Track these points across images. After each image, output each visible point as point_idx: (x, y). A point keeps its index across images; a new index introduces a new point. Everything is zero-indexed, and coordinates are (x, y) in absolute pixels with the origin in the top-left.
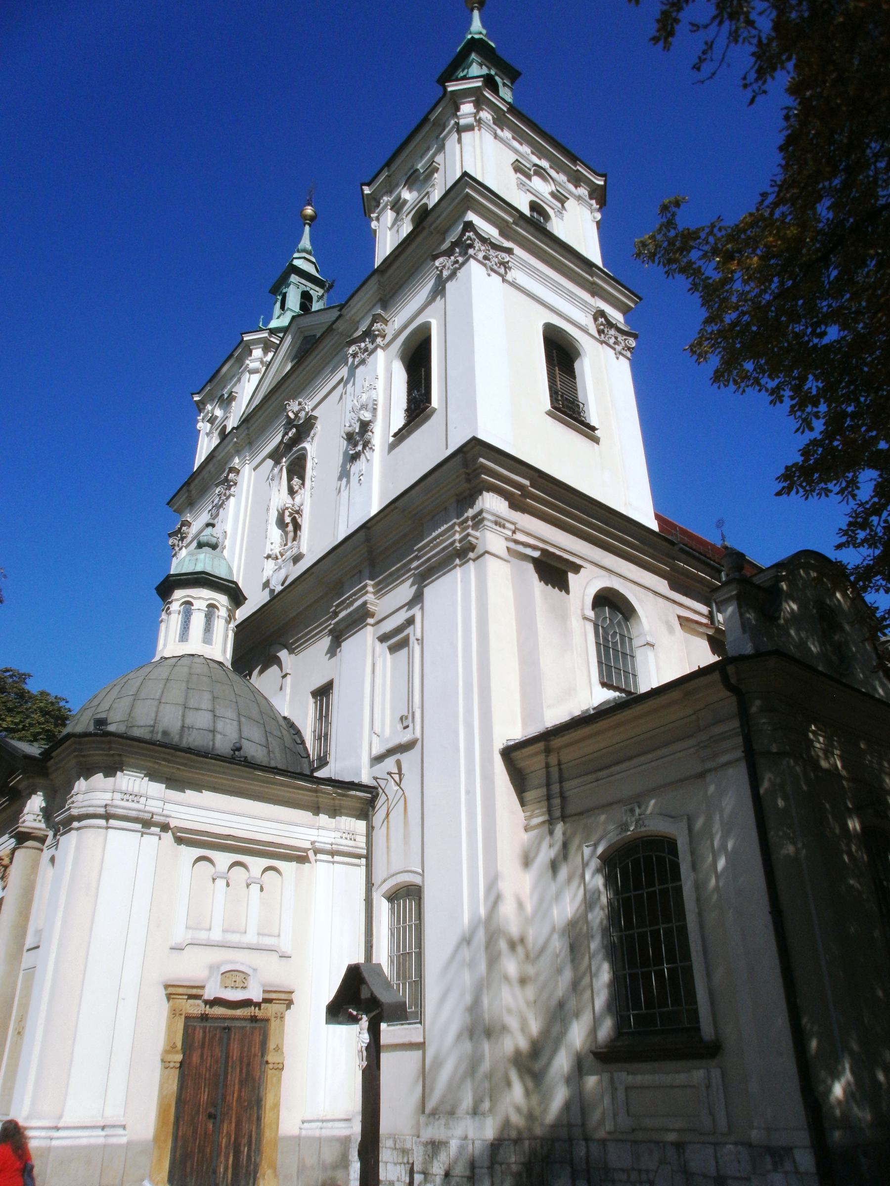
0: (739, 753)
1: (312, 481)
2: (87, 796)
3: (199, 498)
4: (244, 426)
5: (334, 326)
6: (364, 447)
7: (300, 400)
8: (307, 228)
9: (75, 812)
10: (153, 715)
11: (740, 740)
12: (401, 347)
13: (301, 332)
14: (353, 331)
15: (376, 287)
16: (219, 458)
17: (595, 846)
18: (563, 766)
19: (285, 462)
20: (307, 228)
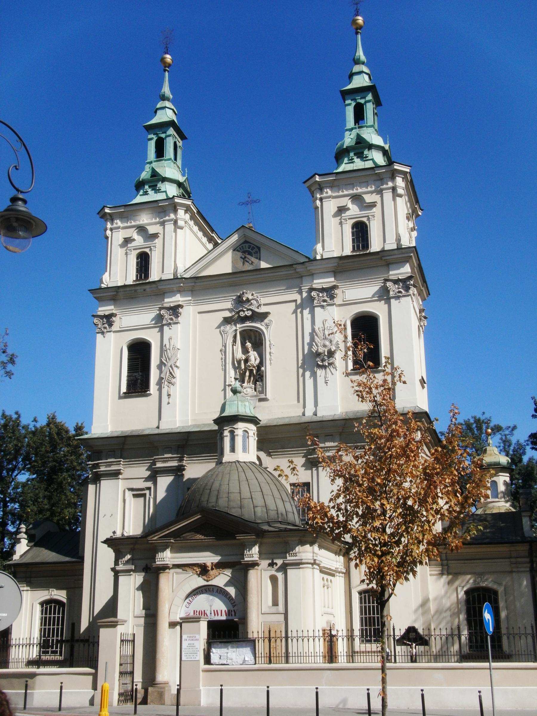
0: (528, 569)
1: (271, 356)
2: (303, 554)
3: (123, 299)
4: (194, 280)
5: (294, 266)
6: (330, 364)
7: (254, 293)
8: (167, 73)
9: (303, 561)
10: (227, 490)
11: (529, 565)
12: (354, 314)
13: (245, 237)
14: (305, 275)
15: (336, 264)
16: (159, 287)
17: (463, 587)
18: (447, 554)
19: (239, 328)
20: (167, 73)
